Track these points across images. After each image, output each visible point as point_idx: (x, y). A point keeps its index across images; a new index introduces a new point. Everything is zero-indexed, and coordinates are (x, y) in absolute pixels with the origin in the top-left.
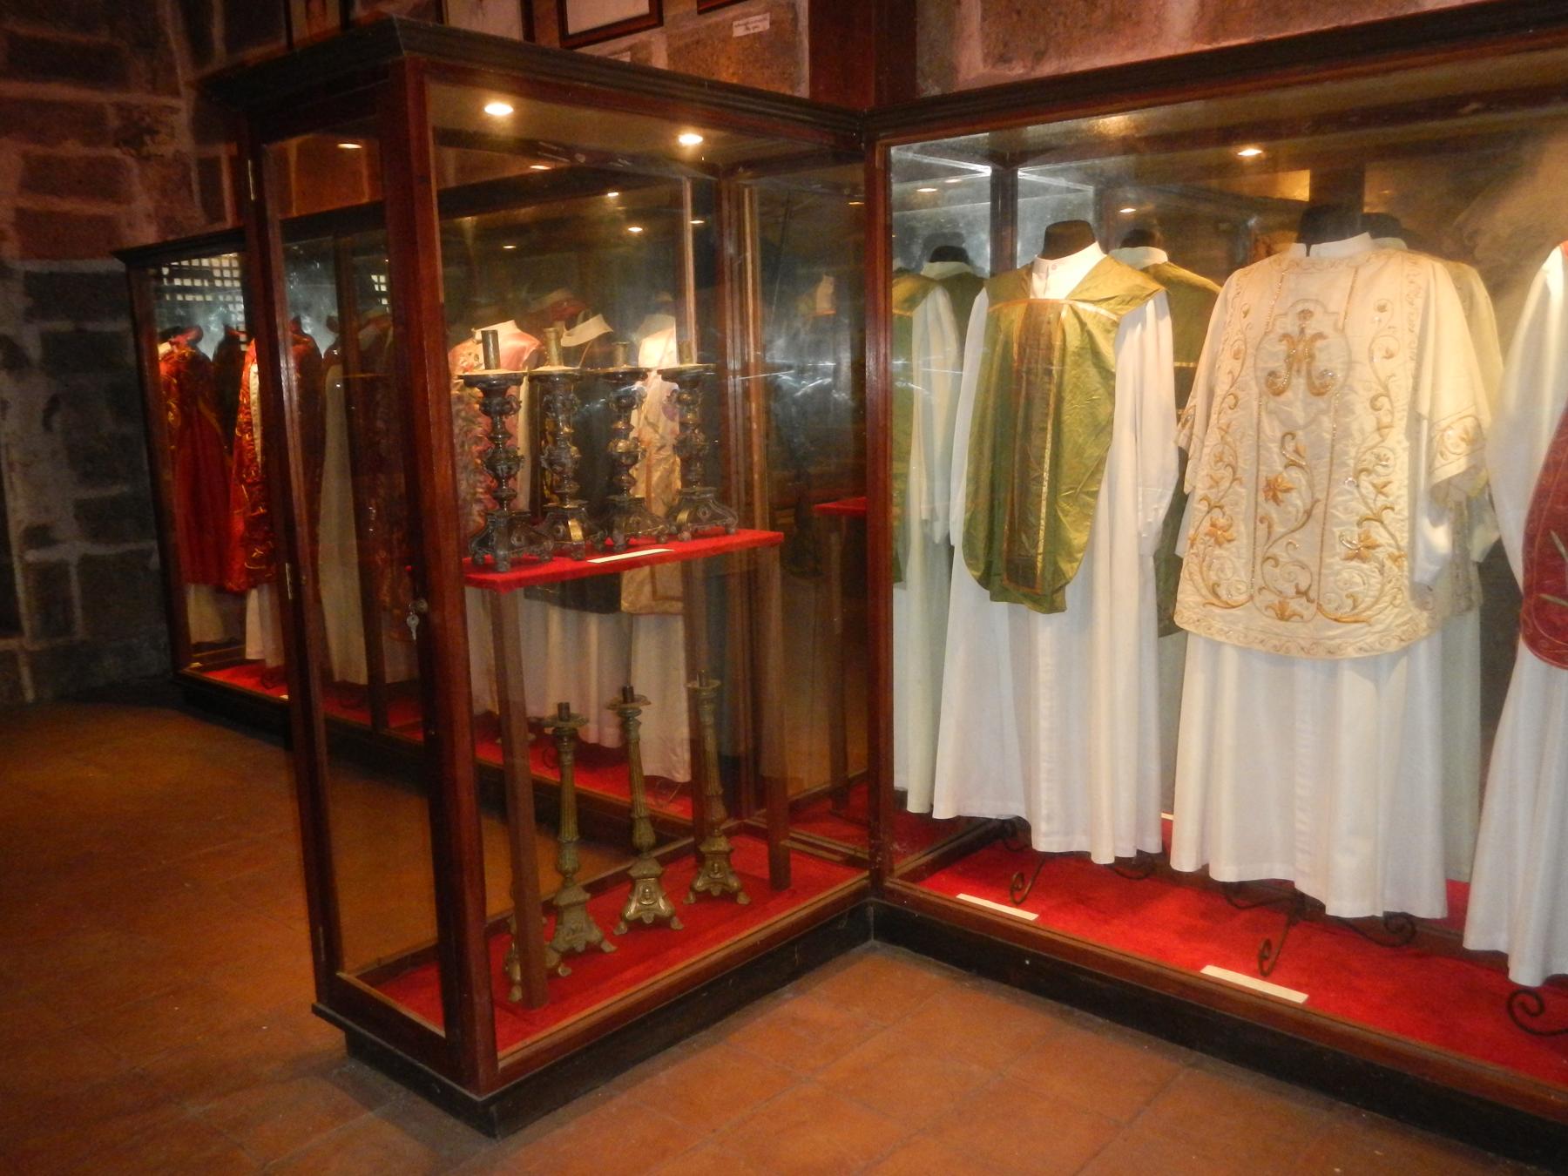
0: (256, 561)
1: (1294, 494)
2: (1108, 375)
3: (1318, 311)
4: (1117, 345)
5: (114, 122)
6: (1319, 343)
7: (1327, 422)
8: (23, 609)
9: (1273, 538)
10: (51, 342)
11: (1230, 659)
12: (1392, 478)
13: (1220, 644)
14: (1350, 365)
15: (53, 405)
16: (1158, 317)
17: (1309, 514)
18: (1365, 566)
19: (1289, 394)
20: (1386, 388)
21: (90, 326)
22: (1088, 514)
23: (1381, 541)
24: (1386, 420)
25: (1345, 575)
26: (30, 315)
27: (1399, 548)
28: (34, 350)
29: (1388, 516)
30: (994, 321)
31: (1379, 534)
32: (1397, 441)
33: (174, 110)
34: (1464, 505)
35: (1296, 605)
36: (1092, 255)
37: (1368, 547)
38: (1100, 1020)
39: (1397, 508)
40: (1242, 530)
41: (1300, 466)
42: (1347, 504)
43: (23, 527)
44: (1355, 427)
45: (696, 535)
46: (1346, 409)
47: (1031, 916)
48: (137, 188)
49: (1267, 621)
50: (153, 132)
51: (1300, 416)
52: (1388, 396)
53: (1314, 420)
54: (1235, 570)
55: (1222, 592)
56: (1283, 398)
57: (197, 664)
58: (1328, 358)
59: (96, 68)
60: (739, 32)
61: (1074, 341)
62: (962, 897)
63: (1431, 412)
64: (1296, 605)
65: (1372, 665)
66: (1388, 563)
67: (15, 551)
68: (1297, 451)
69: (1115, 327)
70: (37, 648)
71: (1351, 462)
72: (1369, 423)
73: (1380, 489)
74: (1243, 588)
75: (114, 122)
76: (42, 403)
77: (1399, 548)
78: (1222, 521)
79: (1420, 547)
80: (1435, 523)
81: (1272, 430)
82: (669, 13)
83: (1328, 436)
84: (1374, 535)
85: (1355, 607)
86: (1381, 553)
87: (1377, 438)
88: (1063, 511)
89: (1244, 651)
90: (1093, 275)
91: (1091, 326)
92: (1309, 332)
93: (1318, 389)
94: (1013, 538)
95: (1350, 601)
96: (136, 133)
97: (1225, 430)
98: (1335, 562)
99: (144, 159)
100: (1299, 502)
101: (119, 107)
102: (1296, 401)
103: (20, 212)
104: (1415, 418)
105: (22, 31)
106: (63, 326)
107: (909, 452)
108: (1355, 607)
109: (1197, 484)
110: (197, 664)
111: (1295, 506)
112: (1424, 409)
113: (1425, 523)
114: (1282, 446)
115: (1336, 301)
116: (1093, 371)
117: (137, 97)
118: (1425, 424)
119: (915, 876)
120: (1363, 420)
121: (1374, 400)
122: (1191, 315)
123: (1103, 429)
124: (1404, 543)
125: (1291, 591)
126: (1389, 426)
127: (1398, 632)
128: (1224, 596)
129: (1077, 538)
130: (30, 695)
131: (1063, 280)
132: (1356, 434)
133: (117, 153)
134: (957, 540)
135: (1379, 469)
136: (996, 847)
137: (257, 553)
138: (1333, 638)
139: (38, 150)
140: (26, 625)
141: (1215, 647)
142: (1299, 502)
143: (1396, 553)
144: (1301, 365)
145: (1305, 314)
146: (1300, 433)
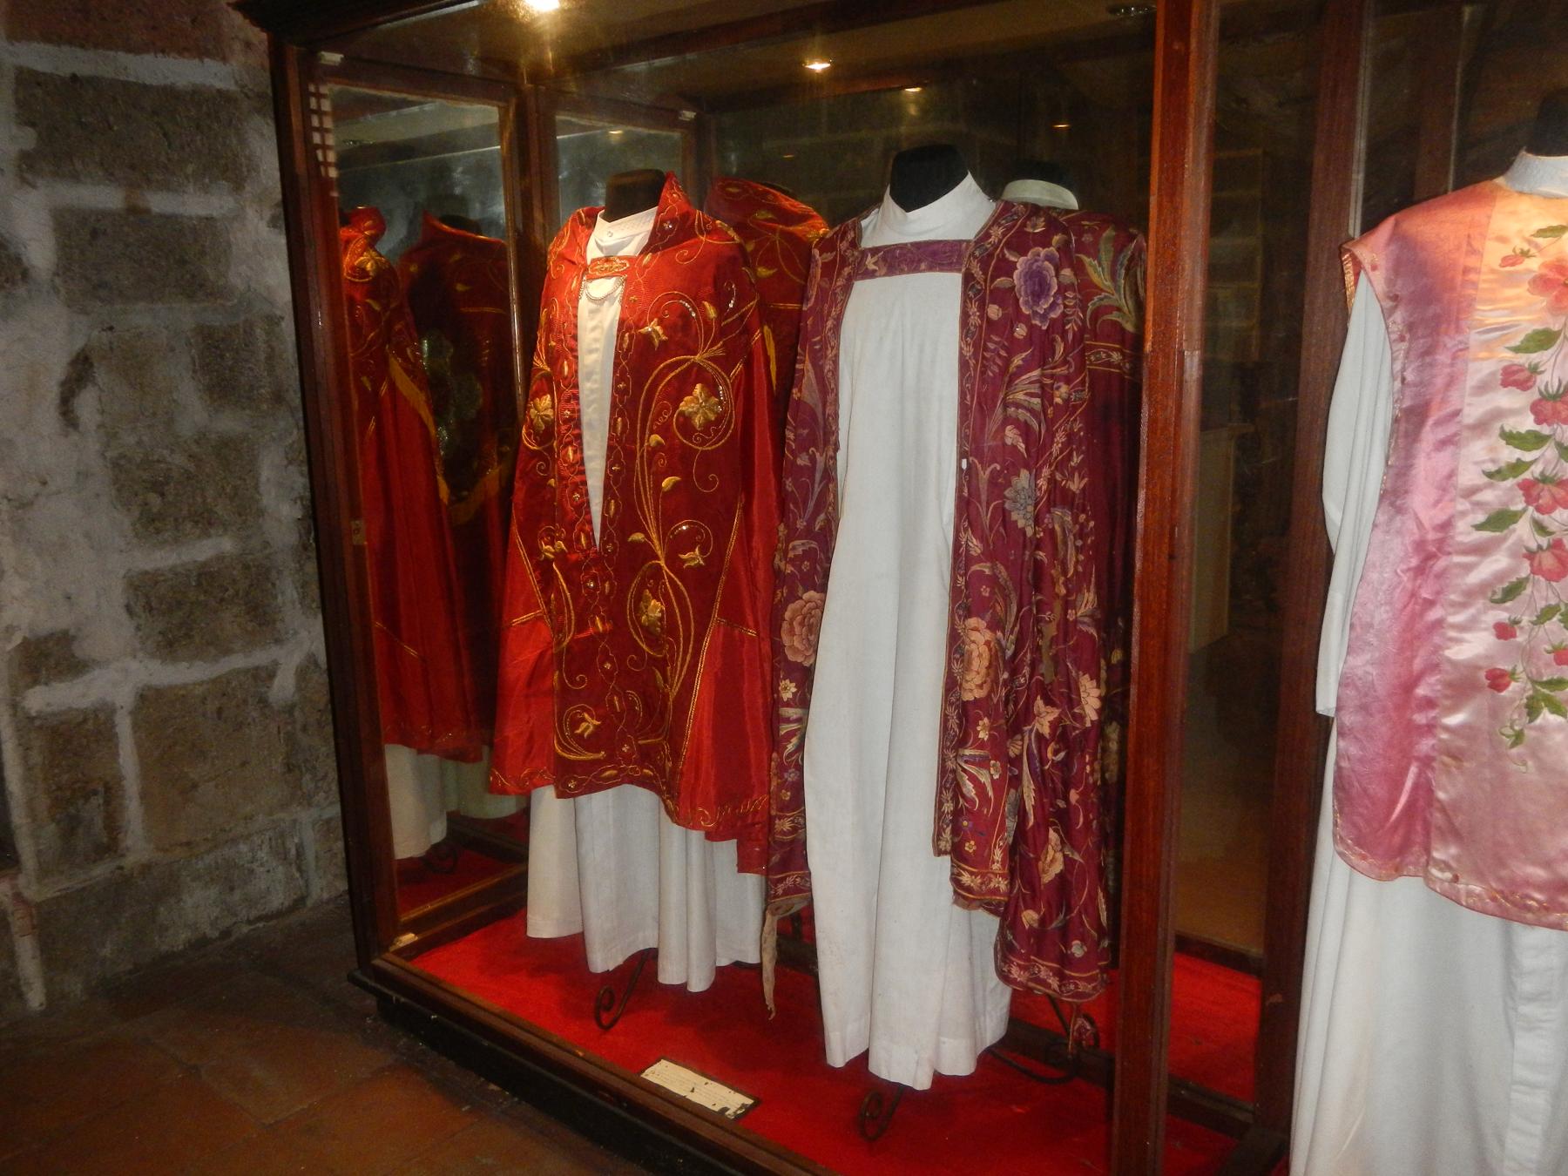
0: (589, 744)
8: (19, 817)
10: (75, 232)
15: (81, 370)
21: (159, 202)
26: (29, 166)
43: (17, 639)
57: (409, 938)
70: (49, 893)
76: (57, 369)
106: (104, 197)
110: (409, 938)
130: (36, 998)
137: (589, 725)
140: (26, 847)
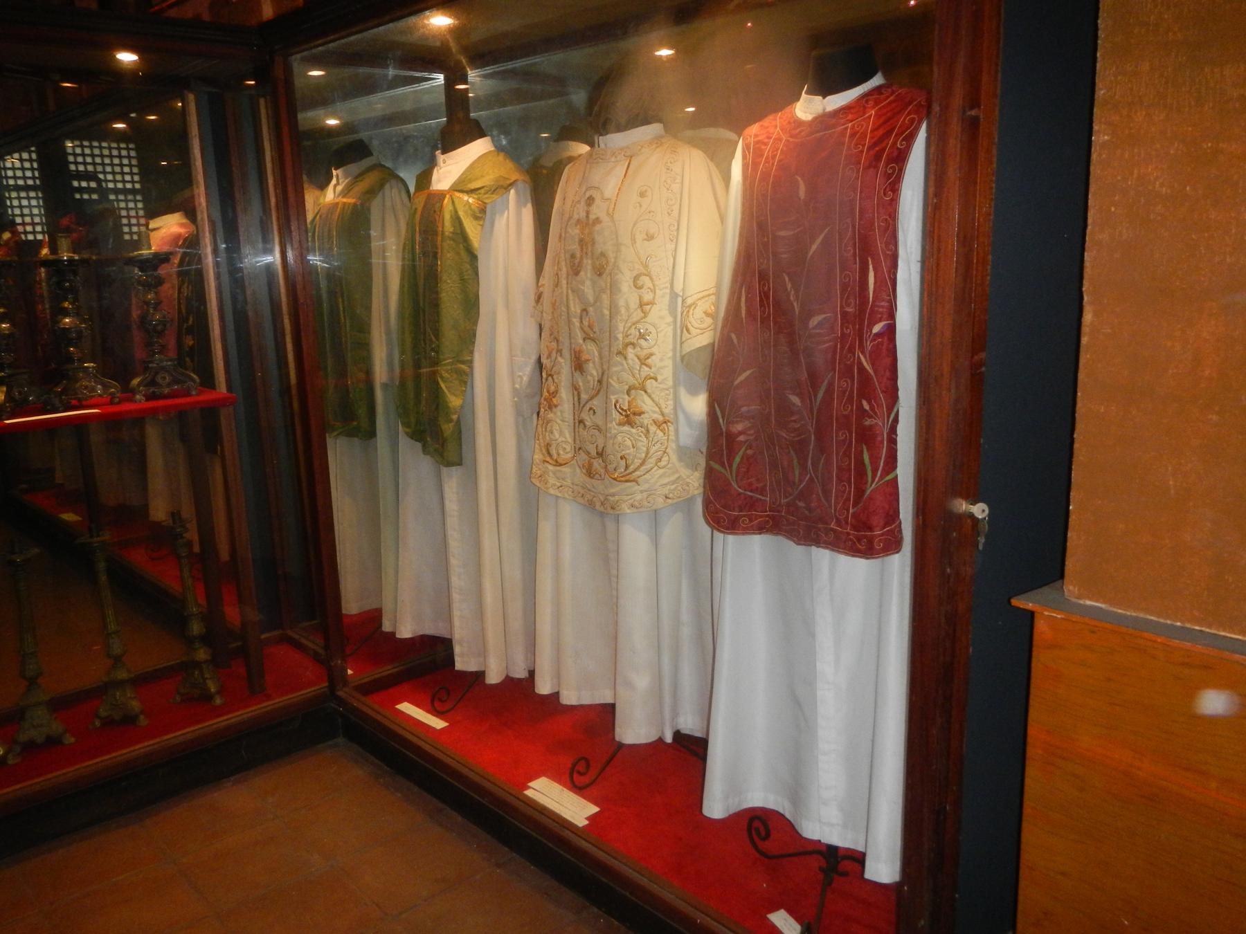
1: (591, 365)
3: (598, 201)
4: (488, 232)
6: (597, 227)
7: (605, 298)
9: (583, 403)
12: (654, 350)
13: (557, 497)
14: (618, 246)
16: (520, 205)
17: (600, 382)
18: (634, 431)
19: (582, 273)
20: (646, 266)
22: (465, 378)
23: (645, 408)
24: (647, 297)
25: (619, 438)
27: (663, 414)
29: (650, 384)
31: (645, 403)
35: (597, 464)
37: (634, 414)
38: (460, 819)
39: (660, 378)
40: (565, 395)
41: (593, 340)
42: (624, 372)
44: (622, 303)
45: (149, 398)
46: (614, 288)
47: (438, 723)
49: (580, 476)
52: (649, 275)
53: (597, 299)
54: (561, 433)
55: (554, 452)
56: (578, 278)
58: (604, 243)
62: (406, 708)
63: (683, 290)
66: (653, 428)
68: (590, 327)
71: (620, 336)
72: (634, 304)
73: (643, 361)
74: (568, 449)
77: (663, 414)
78: (552, 388)
79: (681, 417)
80: (693, 392)
81: (576, 308)
83: (607, 312)
84: (639, 402)
85: (627, 467)
86: (645, 419)
87: (639, 314)
88: (442, 377)
91: (461, 214)
92: (592, 217)
93: (599, 272)
95: (623, 463)
98: (614, 427)
100: (595, 373)
104: (674, 295)
107: (369, 325)
108: (627, 467)
110: (24, 486)
111: (592, 375)
112: (678, 288)
113: (683, 392)
114: (581, 322)
115: (610, 189)
116: (463, 253)
118: (680, 300)
119: (368, 689)
120: (628, 296)
121: (636, 278)
123: (471, 305)
124: (668, 410)
125: (594, 453)
126: (652, 303)
127: (665, 491)
128: (555, 456)
132: (623, 310)
135: (642, 342)
136: (428, 664)
138: (613, 495)
142: (595, 373)
143: (661, 418)
145: (590, 201)
146: (591, 309)
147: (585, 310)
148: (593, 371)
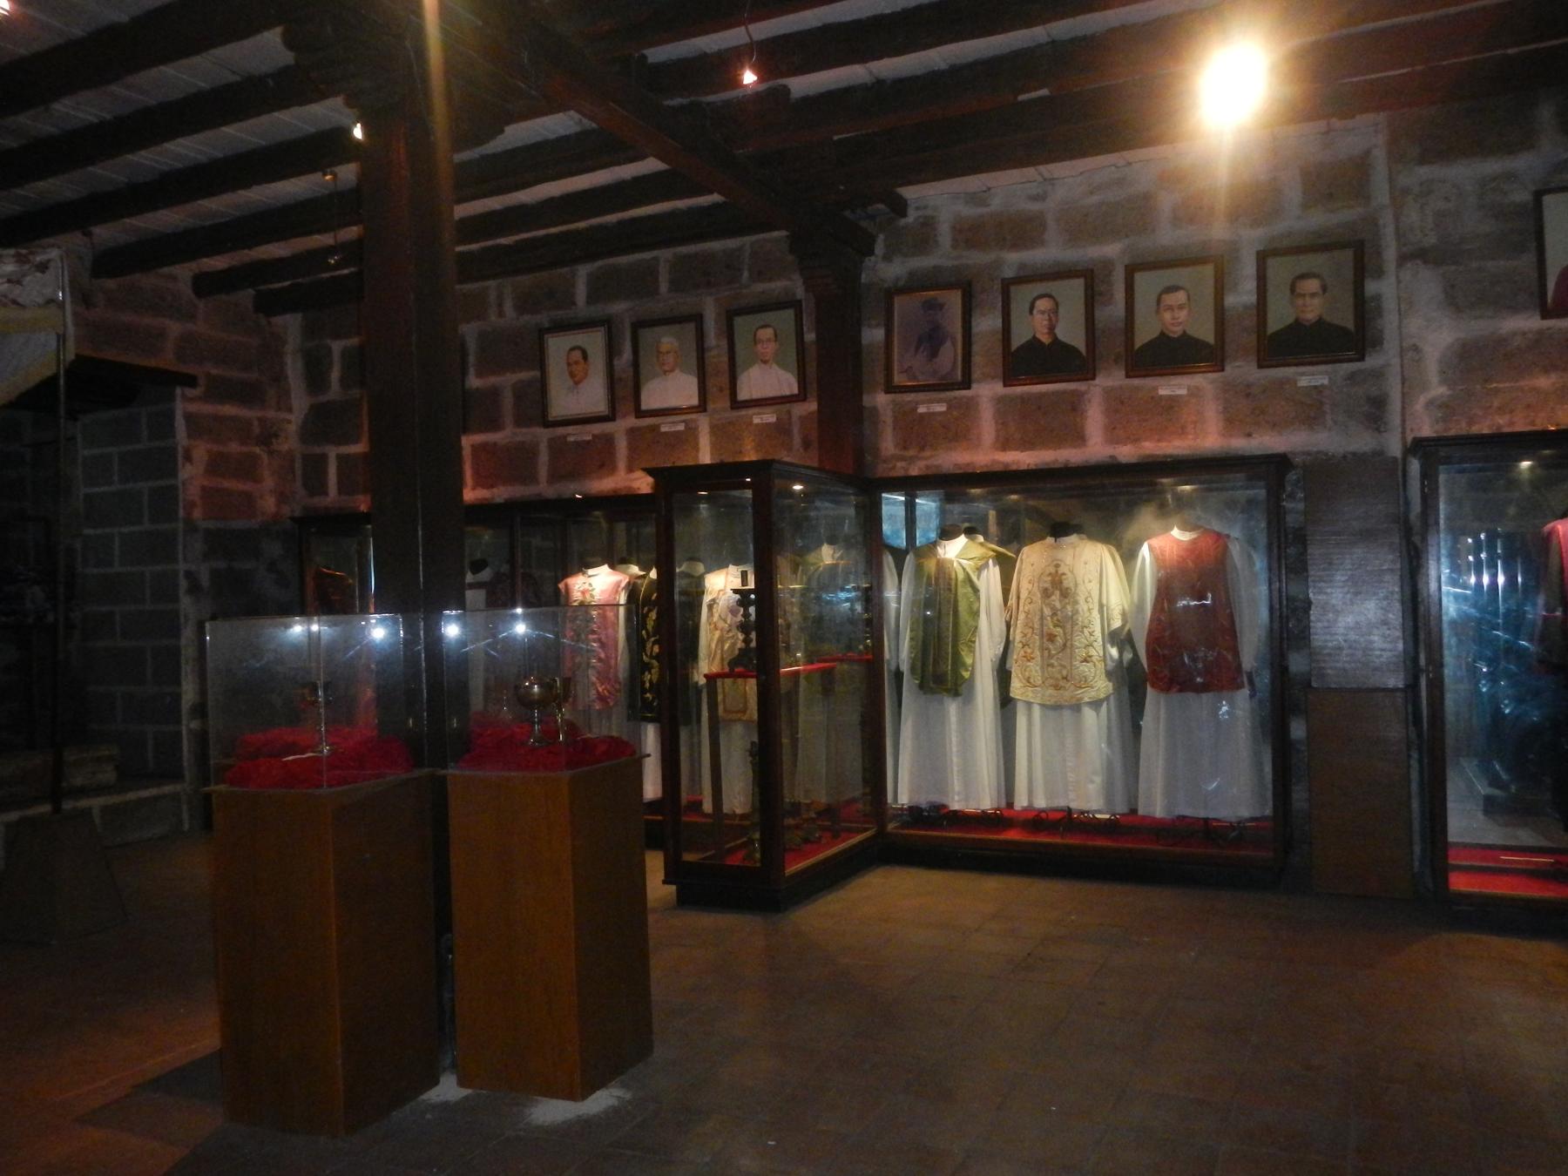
2: (976, 590)
5: (256, 430)
7: (1069, 608)
11: (1037, 711)
14: (1076, 585)
22: (972, 650)
28: (205, 580)
30: (919, 569)
31: (1093, 652)
32: (1096, 614)
33: (289, 422)
34: (1122, 639)
35: (1062, 683)
36: (962, 540)
42: (1079, 641)
46: (1076, 602)
48: (266, 473)
50: (276, 436)
51: (1058, 605)
58: (1068, 582)
59: (248, 394)
60: (756, 420)
61: (961, 576)
64: (1062, 683)
65: (1096, 704)
67: (184, 722)
69: (979, 570)
75: (256, 430)
81: (1047, 612)
82: (710, 406)
89: (1043, 706)
90: (965, 548)
94: (936, 662)
96: (268, 437)
97: (1027, 613)
99: (271, 453)
101: (261, 420)
102: (1055, 598)
103: (203, 488)
104: (1101, 606)
105: (214, 372)
106: (221, 565)
109: (1017, 636)
115: (1069, 560)
117: (271, 414)
120: (1083, 607)
122: (1007, 567)
129: (969, 661)
131: (956, 551)
133: (257, 450)
134: (905, 668)
139: (216, 448)
140: (187, 774)
141: (1029, 704)
144: (1057, 586)
145: (1057, 566)
147: (1054, 614)
148: (1060, 641)
